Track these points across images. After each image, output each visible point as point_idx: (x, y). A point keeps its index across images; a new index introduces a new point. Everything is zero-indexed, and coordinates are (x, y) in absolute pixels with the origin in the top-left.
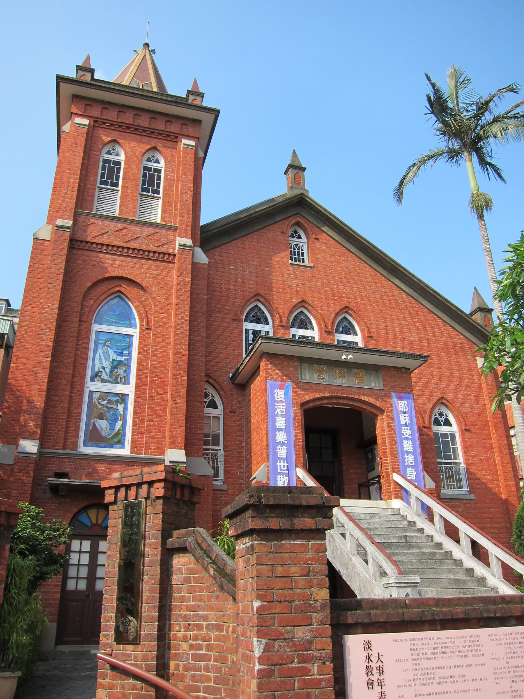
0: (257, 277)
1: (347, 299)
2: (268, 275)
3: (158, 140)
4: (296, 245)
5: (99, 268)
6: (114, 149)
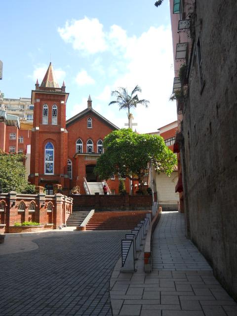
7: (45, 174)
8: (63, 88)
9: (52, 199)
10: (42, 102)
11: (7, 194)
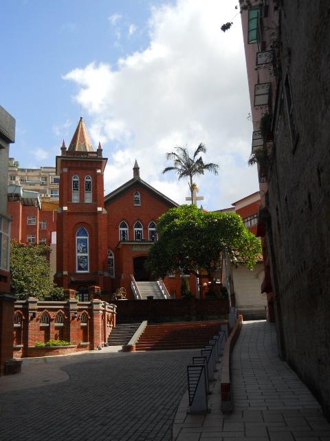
7: (78, 272)
8: (100, 151)
9: (86, 307)
11: (24, 302)
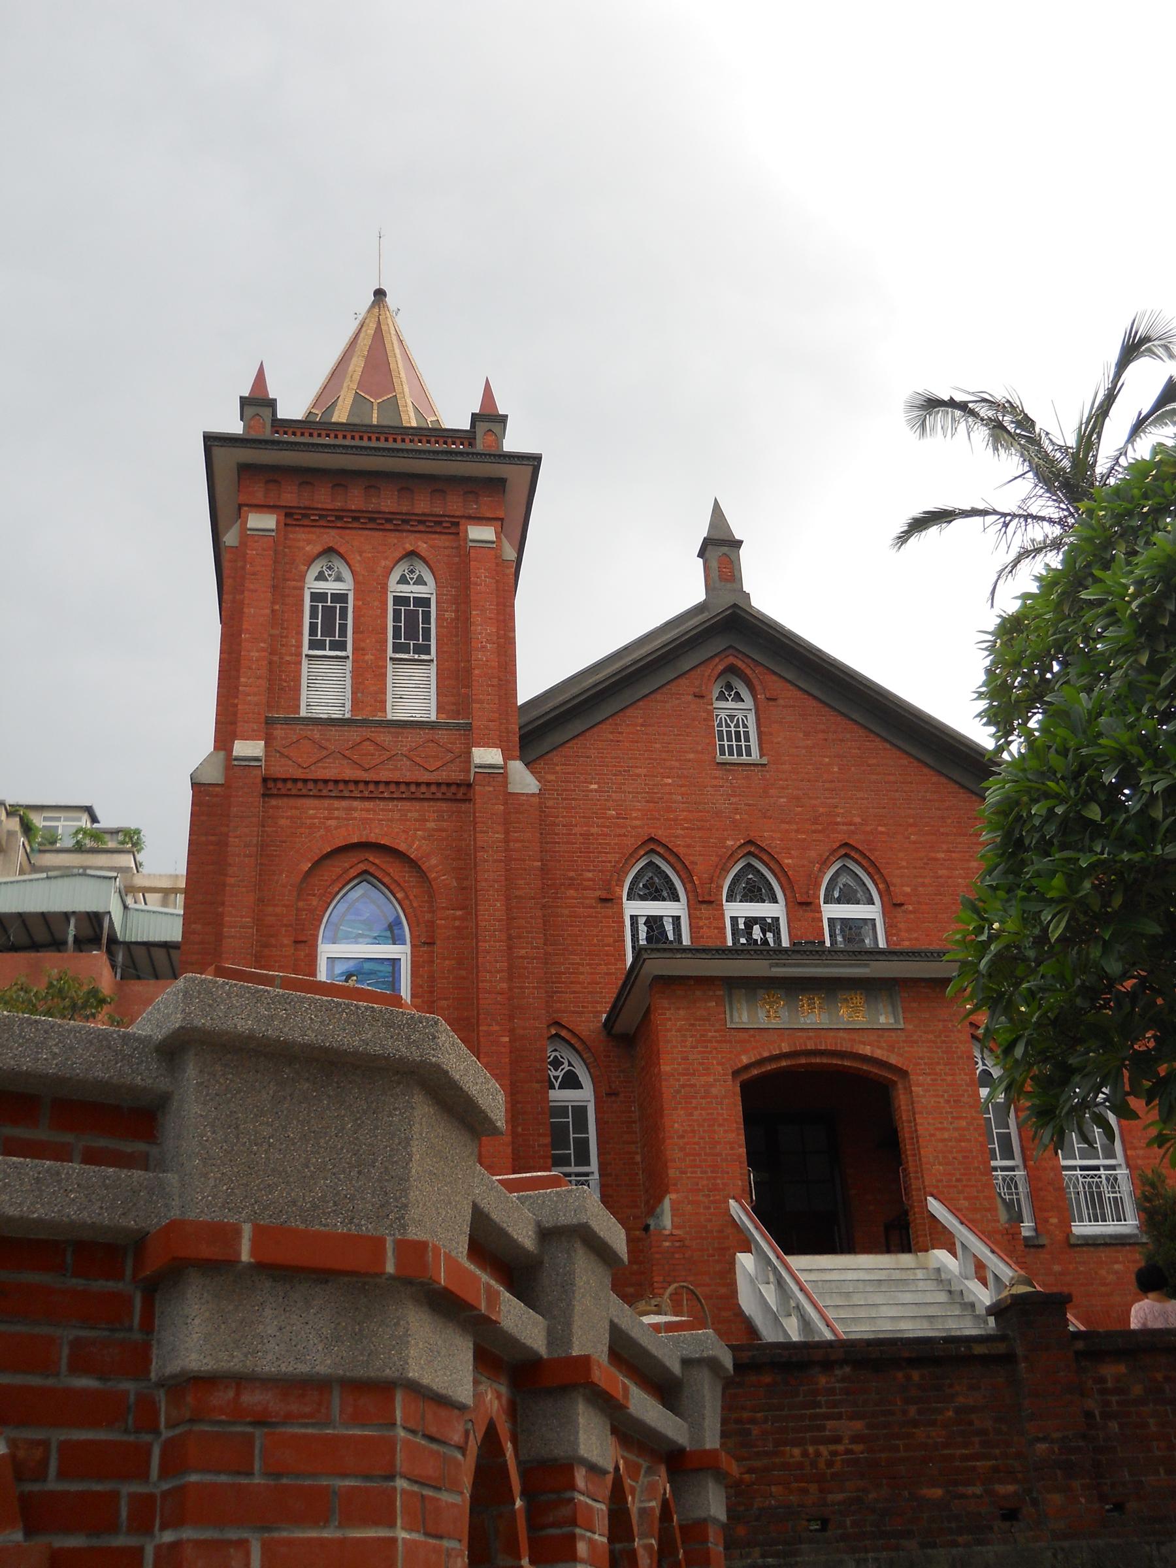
0: (647, 802)
1: (845, 827)
2: (670, 794)
3: (418, 535)
4: (732, 717)
5: (322, 832)
6: (330, 568)
8: (490, 419)
10: (300, 535)
